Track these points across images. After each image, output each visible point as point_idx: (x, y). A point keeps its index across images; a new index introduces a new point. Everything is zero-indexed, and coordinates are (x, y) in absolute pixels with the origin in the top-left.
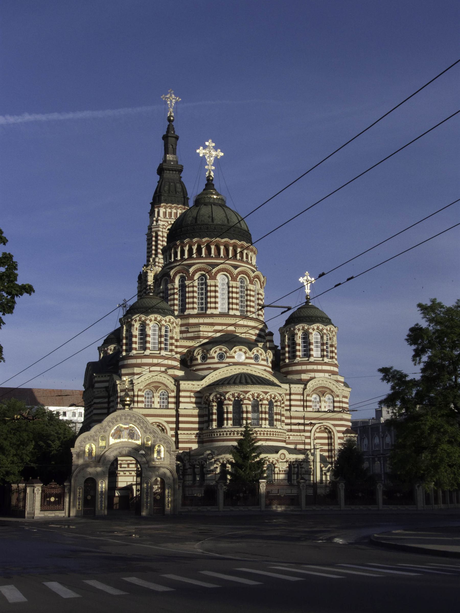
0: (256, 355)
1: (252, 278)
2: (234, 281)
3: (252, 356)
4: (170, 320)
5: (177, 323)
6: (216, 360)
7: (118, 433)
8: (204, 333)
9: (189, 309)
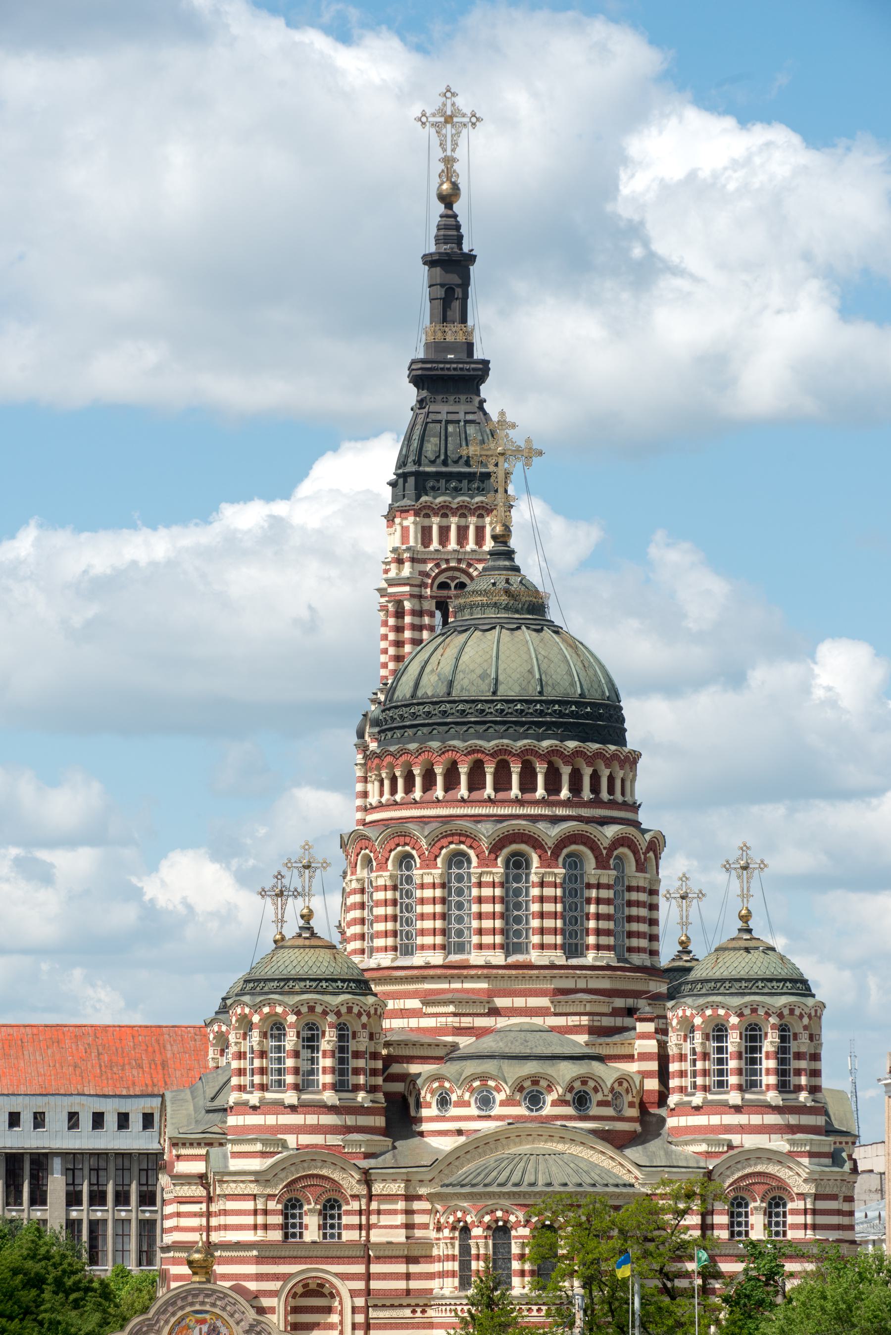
0: (580, 1091)
1: (604, 852)
2: (549, 866)
3: (569, 1097)
4: (350, 1010)
5: (372, 1012)
6: (473, 1111)
7: (185, 1332)
8: (464, 1019)
9: (423, 947)
